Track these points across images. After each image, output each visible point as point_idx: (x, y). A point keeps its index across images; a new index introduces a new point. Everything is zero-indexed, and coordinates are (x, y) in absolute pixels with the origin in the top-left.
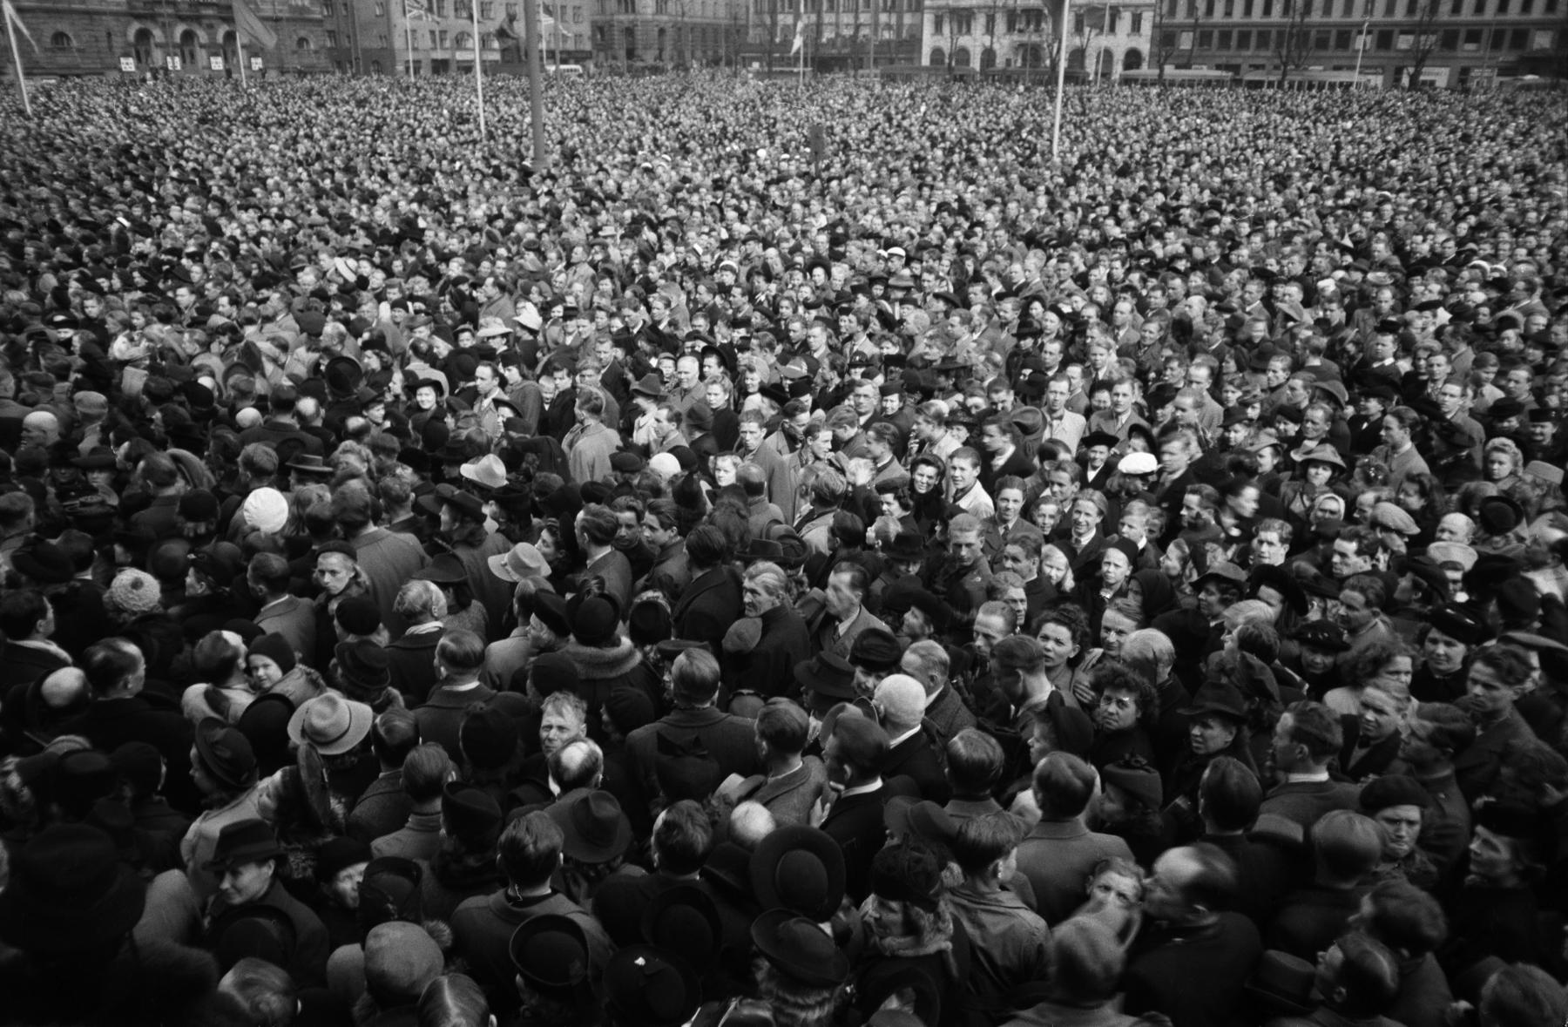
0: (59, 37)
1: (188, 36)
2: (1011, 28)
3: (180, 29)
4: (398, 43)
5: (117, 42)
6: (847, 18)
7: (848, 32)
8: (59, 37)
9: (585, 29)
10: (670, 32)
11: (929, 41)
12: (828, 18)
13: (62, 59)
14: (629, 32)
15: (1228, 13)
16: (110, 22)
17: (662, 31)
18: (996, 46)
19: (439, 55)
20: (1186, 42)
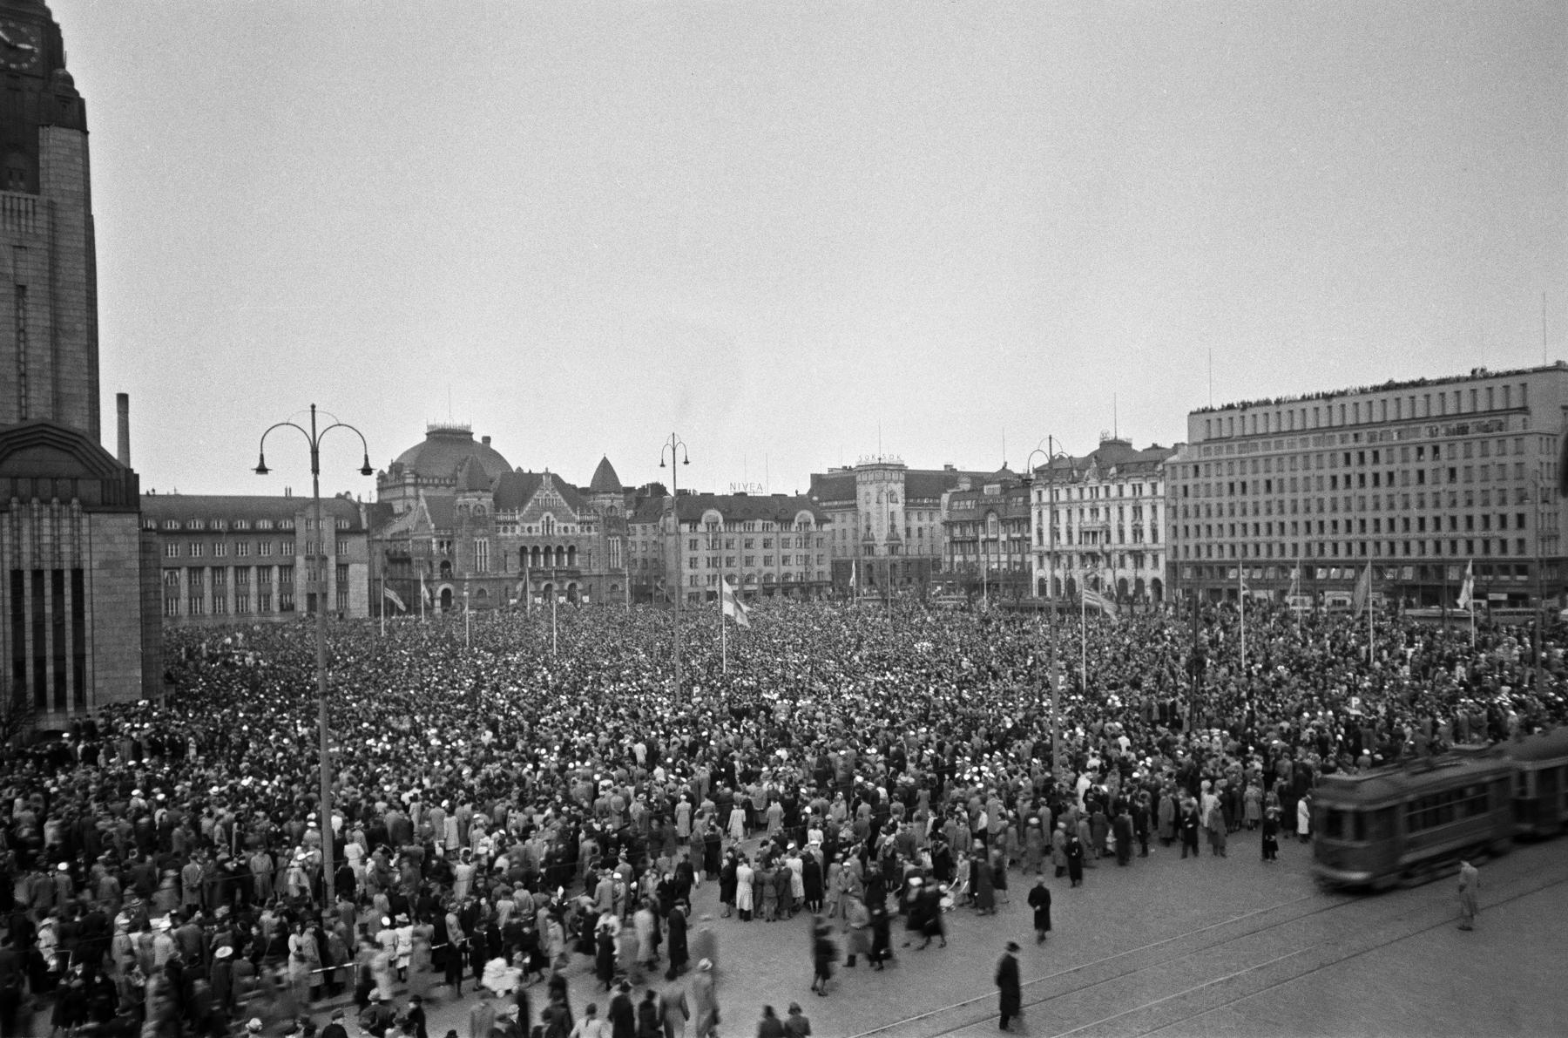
0: (481, 591)
1: (573, 585)
2: (1083, 565)
3: (543, 586)
4: (686, 583)
5: (510, 592)
6: (993, 558)
7: (1005, 566)
8: (481, 591)
9: (826, 568)
10: (900, 567)
11: (1037, 573)
12: (983, 558)
13: (481, 601)
14: (870, 567)
15: (1210, 555)
16: (508, 583)
17: (894, 566)
18: (1075, 577)
19: (710, 589)
20: (1188, 574)
